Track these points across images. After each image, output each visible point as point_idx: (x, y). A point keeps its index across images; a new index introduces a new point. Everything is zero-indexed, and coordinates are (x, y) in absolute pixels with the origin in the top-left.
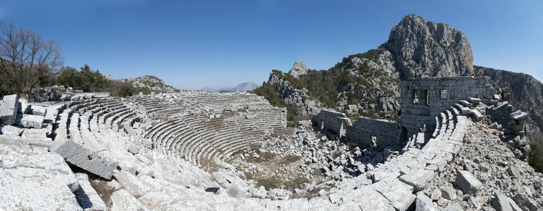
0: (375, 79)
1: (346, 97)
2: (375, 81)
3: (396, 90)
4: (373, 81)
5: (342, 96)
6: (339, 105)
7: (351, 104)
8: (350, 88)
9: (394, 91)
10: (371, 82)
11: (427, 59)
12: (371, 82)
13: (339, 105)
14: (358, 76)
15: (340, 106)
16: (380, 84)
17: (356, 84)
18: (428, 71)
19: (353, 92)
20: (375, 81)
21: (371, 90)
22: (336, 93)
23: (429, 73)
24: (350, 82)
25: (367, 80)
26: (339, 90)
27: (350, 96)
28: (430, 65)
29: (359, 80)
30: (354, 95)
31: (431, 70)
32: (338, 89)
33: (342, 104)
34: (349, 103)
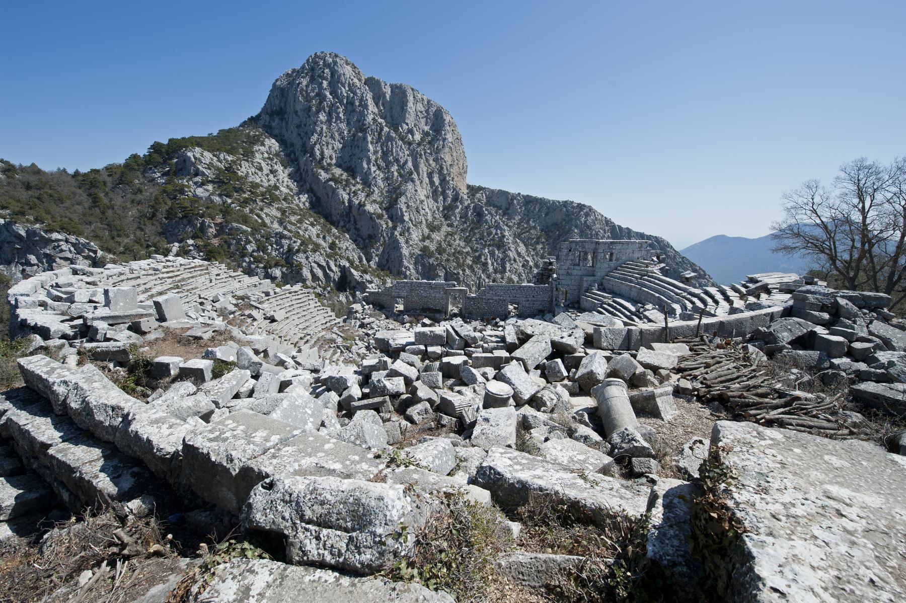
0: (266, 210)
2: (267, 215)
3: (318, 235)
4: (264, 216)
8: (203, 229)
9: (315, 239)
10: (259, 216)
11: (373, 169)
12: (259, 216)
14: (217, 199)
16: (281, 222)
17: (219, 219)
18: (376, 196)
19: (215, 242)
20: (267, 215)
21: (266, 239)
23: (379, 199)
25: (247, 210)
27: (210, 251)
28: (381, 183)
31: (382, 193)
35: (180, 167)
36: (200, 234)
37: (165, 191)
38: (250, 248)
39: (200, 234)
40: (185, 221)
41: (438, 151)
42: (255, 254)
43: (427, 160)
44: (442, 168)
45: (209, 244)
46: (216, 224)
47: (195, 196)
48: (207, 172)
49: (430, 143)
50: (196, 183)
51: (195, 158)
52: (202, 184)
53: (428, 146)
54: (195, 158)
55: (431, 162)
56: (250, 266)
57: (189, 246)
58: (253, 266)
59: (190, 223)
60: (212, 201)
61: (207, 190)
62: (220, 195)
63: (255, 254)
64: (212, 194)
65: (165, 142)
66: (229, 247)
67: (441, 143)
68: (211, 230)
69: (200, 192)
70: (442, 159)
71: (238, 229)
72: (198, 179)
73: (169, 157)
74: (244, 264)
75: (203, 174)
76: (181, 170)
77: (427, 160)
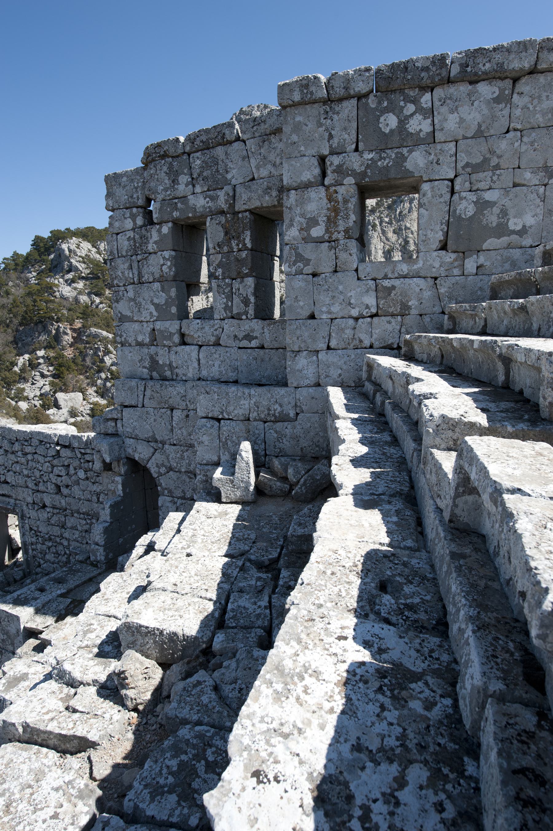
1: (45, 369)
5: (33, 365)
6: (20, 396)
7: (66, 391)
8: (57, 338)
13: (20, 396)
15: (27, 399)
17: (78, 324)
19: (69, 353)
22: (10, 357)
24: (58, 320)
26: (20, 344)
27: (60, 365)
29: (87, 313)
30: (74, 360)
32: (15, 342)
33: (31, 391)
34: (56, 388)
35: (55, 263)
36: (54, 343)
37: (29, 294)
38: (108, 360)
39: (54, 343)
40: (40, 326)
41: (402, 217)
42: (114, 368)
43: (384, 232)
44: (407, 242)
45: (63, 356)
46: (74, 330)
47: (62, 297)
48: (81, 266)
49: (389, 207)
50: (66, 281)
51: (70, 251)
52: (73, 281)
53: (386, 212)
54: (70, 251)
55: (390, 235)
56: (104, 385)
57: (38, 358)
58: (108, 384)
59: (45, 329)
60: (76, 300)
61: (75, 289)
62: (89, 294)
63: (114, 368)
64: (80, 293)
65: (46, 234)
66: (84, 360)
67: (407, 205)
68: (66, 338)
69: (66, 291)
70: (407, 228)
71: (96, 336)
72: (70, 276)
73: (47, 252)
74: (99, 382)
75: (77, 269)
76: (56, 267)
77: (384, 232)
